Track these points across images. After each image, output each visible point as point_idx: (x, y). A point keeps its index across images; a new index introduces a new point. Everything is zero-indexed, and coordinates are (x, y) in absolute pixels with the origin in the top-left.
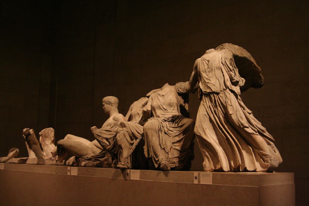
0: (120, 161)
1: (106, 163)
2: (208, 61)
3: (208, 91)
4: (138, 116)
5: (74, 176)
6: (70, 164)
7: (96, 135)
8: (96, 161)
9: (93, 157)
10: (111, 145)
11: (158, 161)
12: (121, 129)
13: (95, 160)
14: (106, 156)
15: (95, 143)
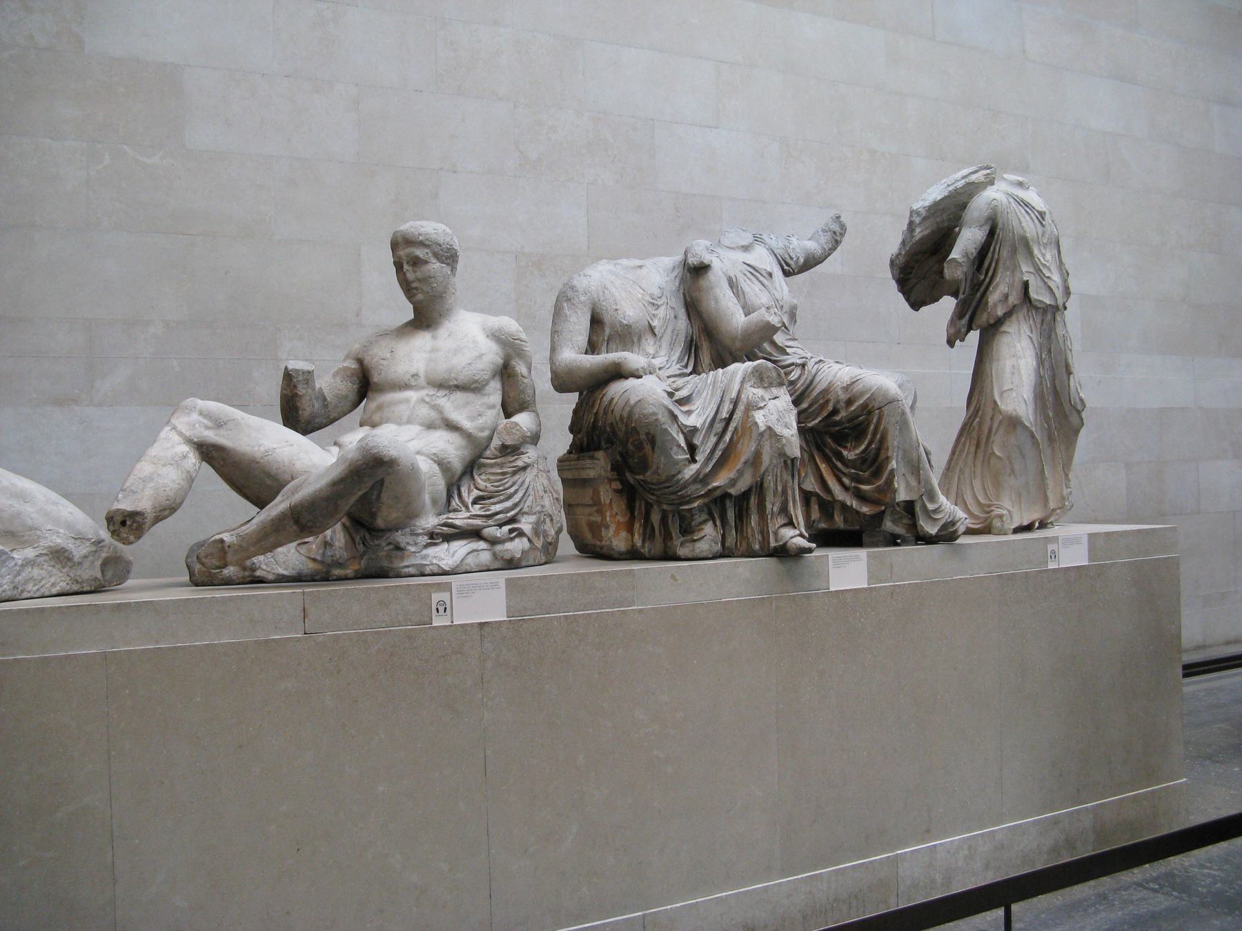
0: (790, 524)
1: (539, 543)
2: (1040, 213)
3: (1048, 301)
4: (651, 340)
5: (482, 625)
6: (258, 573)
7: (666, 414)
8: (512, 539)
9: (490, 522)
10: (700, 457)
11: (935, 511)
12: (760, 392)
13: (511, 531)
14: (526, 509)
15: (434, 451)
